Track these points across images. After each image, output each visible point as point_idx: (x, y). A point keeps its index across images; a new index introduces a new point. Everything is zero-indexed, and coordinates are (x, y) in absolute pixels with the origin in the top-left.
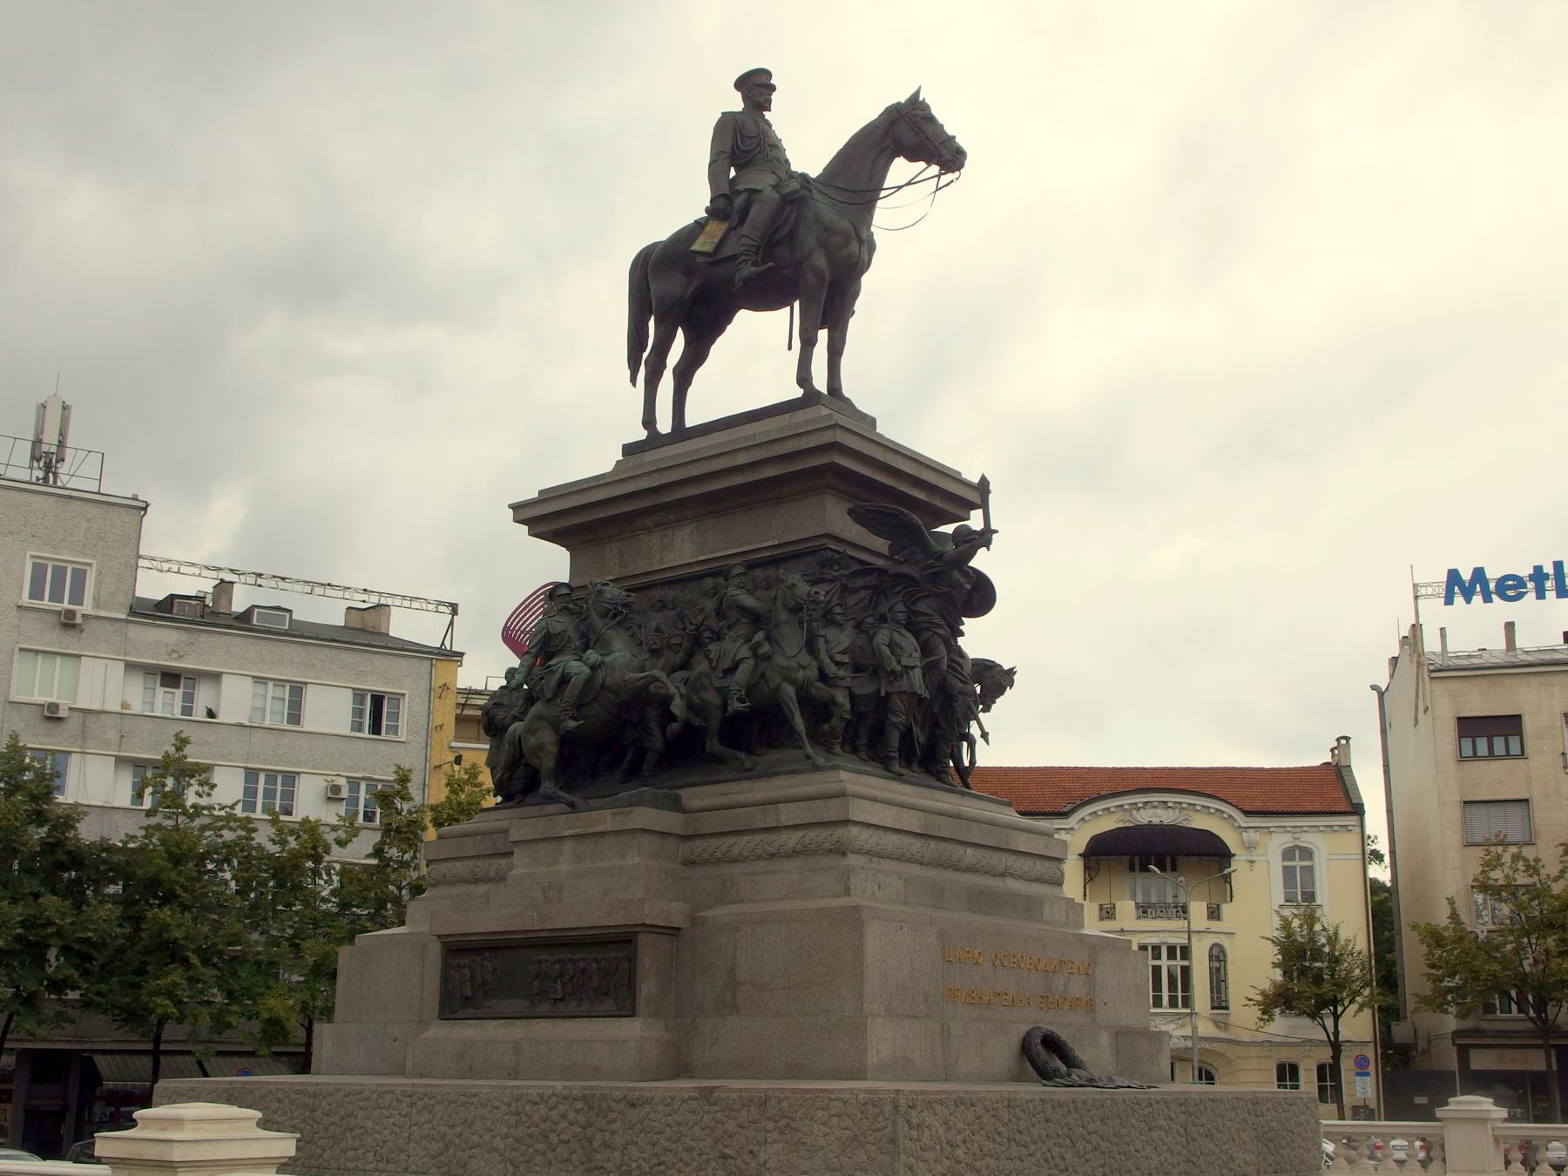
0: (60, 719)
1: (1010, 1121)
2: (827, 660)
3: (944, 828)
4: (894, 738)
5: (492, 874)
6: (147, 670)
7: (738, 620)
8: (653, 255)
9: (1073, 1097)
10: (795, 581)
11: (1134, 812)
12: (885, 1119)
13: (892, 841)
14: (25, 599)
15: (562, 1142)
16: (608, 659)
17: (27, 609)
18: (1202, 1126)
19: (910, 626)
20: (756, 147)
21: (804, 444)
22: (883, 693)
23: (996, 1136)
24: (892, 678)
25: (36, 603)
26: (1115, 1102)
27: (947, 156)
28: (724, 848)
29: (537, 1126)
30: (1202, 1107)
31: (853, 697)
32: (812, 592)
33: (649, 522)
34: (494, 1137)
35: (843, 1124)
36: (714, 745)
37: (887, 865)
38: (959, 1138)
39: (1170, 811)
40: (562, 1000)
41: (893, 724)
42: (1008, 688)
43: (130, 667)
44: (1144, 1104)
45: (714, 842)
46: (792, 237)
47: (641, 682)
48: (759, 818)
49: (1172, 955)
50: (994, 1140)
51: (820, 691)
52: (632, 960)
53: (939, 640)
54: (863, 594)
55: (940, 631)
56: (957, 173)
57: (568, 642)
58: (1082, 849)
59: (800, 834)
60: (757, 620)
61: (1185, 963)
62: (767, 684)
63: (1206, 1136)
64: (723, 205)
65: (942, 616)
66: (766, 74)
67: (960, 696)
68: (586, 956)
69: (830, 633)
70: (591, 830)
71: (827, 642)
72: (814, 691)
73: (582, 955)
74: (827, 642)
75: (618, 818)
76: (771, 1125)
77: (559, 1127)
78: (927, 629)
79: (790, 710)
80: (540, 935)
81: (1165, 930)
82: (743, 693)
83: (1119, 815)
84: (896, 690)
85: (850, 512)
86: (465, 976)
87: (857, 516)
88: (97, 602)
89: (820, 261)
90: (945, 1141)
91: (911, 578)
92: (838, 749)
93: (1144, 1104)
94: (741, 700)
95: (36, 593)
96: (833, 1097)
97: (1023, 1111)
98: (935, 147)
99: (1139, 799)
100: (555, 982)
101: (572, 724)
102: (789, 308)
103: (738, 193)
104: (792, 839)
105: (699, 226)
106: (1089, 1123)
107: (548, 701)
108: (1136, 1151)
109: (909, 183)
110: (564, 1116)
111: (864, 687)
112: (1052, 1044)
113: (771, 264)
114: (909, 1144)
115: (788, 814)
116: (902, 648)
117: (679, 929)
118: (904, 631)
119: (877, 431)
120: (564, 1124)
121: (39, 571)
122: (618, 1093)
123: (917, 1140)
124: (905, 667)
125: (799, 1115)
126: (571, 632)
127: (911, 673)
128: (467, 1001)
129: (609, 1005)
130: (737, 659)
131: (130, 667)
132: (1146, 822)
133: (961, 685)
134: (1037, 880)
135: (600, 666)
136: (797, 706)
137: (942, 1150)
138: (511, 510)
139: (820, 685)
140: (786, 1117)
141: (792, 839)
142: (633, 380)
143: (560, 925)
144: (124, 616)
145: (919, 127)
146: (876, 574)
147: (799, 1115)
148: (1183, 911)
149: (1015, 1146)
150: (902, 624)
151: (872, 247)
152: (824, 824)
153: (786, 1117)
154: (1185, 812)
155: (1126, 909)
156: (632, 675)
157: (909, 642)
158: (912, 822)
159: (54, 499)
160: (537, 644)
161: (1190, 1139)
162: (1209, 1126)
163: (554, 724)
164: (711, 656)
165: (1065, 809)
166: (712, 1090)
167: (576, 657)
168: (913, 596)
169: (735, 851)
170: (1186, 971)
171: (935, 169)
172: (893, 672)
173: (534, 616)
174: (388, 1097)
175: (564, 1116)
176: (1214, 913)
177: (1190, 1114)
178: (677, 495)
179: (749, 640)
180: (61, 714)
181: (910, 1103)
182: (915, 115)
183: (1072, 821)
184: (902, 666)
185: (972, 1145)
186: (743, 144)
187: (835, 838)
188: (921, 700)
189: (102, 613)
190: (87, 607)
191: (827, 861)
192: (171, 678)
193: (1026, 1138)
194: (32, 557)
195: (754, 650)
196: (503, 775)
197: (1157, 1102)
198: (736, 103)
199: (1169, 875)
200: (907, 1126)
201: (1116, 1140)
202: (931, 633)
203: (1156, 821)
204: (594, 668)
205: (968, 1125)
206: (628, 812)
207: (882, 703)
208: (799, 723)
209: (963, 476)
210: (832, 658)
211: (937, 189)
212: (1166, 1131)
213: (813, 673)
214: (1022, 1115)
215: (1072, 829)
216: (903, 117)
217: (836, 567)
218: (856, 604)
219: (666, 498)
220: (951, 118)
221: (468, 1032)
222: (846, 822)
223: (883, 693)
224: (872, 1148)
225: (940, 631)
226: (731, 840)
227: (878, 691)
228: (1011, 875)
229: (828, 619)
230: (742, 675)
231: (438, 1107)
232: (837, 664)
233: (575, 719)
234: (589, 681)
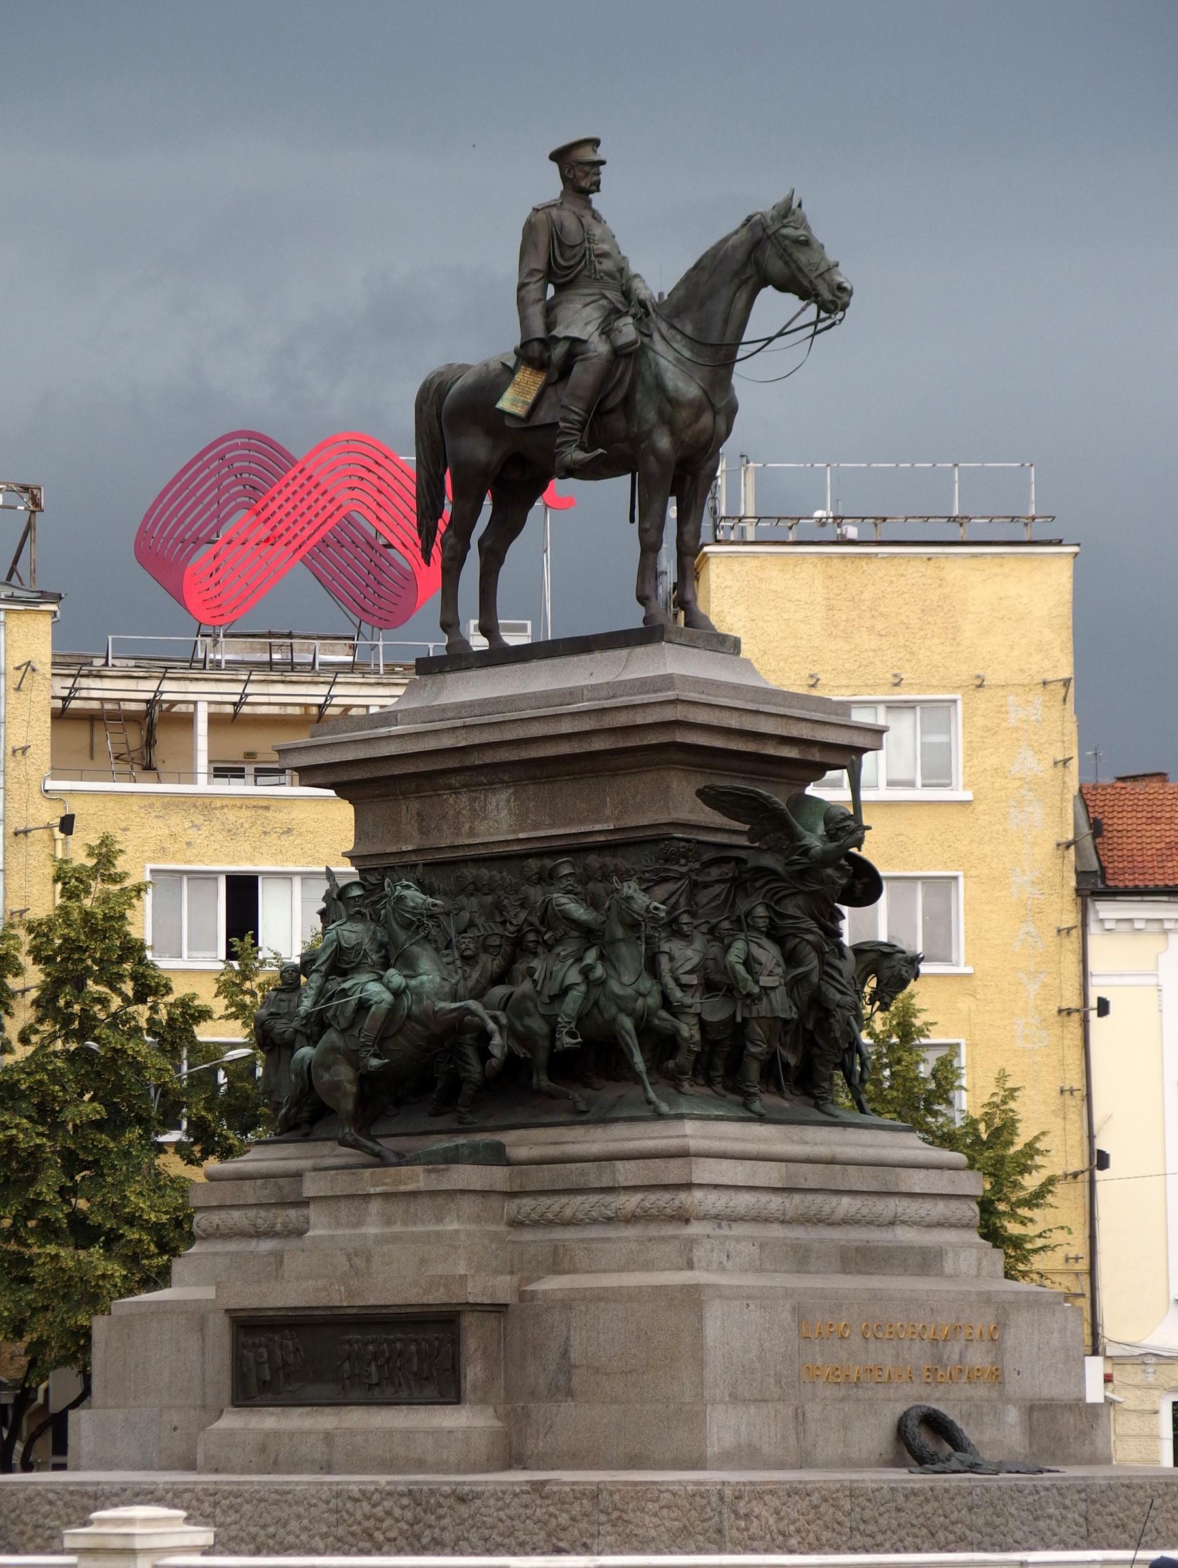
1: (852, 1510)
2: (671, 984)
3: (812, 1176)
5: (278, 1227)
7: (566, 934)
8: (451, 391)
9: (932, 1484)
10: (631, 892)
12: (712, 1510)
13: (743, 1202)
15: (388, 1540)
16: (413, 982)
18: (1111, 1515)
19: (775, 935)
20: (580, 262)
21: (640, 719)
22: (739, 1019)
23: (836, 1526)
24: (748, 1002)
26: (987, 1490)
28: (556, 1208)
29: (360, 1524)
30: (1110, 1494)
31: (703, 1025)
32: (652, 906)
33: (454, 781)
34: (312, 1537)
35: (673, 1515)
36: (542, 1081)
37: (739, 1230)
38: (792, 1528)
40: (377, 1384)
41: (752, 1055)
42: (913, 980)
44: (1027, 1492)
45: (545, 1201)
46: (628, 402)
47: (454, 1014)
48: (595, 1176)
50: (834, 1530)
52: (456, 1342)
53: (808, 948)
54: (717, 889)
55: (810, 937)
59: (639, 1197)
62: (601, 1013)
63: (1117, 1527)
65: (814, 918)
67: (839, 1010)
68: (403, 1336)
69: (675, 947)
70: (402, 1188)
71: (672, 959)
72: (657, 1022)
73: (399, 1335)
74: (672, 959)
75: (433, 1176)
76: (603, 1518)
77: (385, 1525)
78: (795, 936)
80: (349, 1311)
82: (573, 1025)
84: (755, 1015)
87: (708, 796)
89: (664, 442)
90: (776, 1531)
91: (774, 872)
93: (1027, 1492)
94: (572, 1035)
96: (662, 1488)
97: (869, 1500)
100: (369, 1365)
101: (375, 1062)
102: (630, 475)
103: (556, 340)
104: (631, 1202)
105: (509, 372)
106: (952, 1512)
107: (343, 1031)
108: (1016, 1542)
109: (780, 334)
111: (716, 1011)
112: (936, 1424)
114: (735, 1533)
115: (626, 1173)
116: (761, 964)
117: (506, 1305)
118: (765, 942)
120: (389, 1522)
122: (447, 1488)
123: (744, 1530)
124: (765, 988)
125: (631, 1506)
126: (367, 945)
127: (772, 995)
129: (430, 1391)
130: (567, 983)
133: (838, 996)
134: (939, 1225)
135: (404, 991)
136: (636, 1041)
137: (773, 1540)
139: (663, 1014)
140: (618, 1509)
141: (631, 1202)
142: (427, 555)
143: (372, 1302)
145: (790, 255)
146: (733, 863)
147: (631, 1506)
149: (858, 1536)
150: (762, 932)
152: (665, 1187)
153: (618, 1509)
157: (768, 954)
158: (769, 1174)
160: (326, 961)
161: (1092, 1529)
162: (1121, 1515)
163: (353, 1059)
164: (536, 977)
166: (544, 1483)
167: (374, 976)
168: (776, 893)
169: (568, 1212)
172: (749, 995)
173: (201, 507)
174: (187, 1496)
175: (389, 1513)
177: (1093, 1502)
178: (489, 758)
179: (579, 959)
181: (737, 1494)
182: (786, 237)
184: (761, 987)
185: (808, 1535)
186: (562, 256)
187: (677, 1203)
191: (669, 1230)
193: (872, 1528)
195: (586, 972)
196: (289, 1110)
197: (1047, 1489)
198: (550, 187)
200: (733, 1516)
201: (989, 1530)
202: (798, 940)
204: (397, 993)
205: (803, 1514)
206: (447, 1170)
207: (738, 1030)
210: (676, 980)
212: (1057, 1521)
213: (654, 1000)
214: (868, 1504)
216: (769, 237)
217: (683, 861)
218: (708, 903)
219: (476, 760)
222: (689, 1186)
223: (739, 1019)
224: (701, 1538)
225: (810, 937)
226: (564, 1200)
227: (734, 1015)
228: (904, 1222)
229: (674, 929)
231: (247, 1507)
232: (684, 987)
234: (393, 1010)
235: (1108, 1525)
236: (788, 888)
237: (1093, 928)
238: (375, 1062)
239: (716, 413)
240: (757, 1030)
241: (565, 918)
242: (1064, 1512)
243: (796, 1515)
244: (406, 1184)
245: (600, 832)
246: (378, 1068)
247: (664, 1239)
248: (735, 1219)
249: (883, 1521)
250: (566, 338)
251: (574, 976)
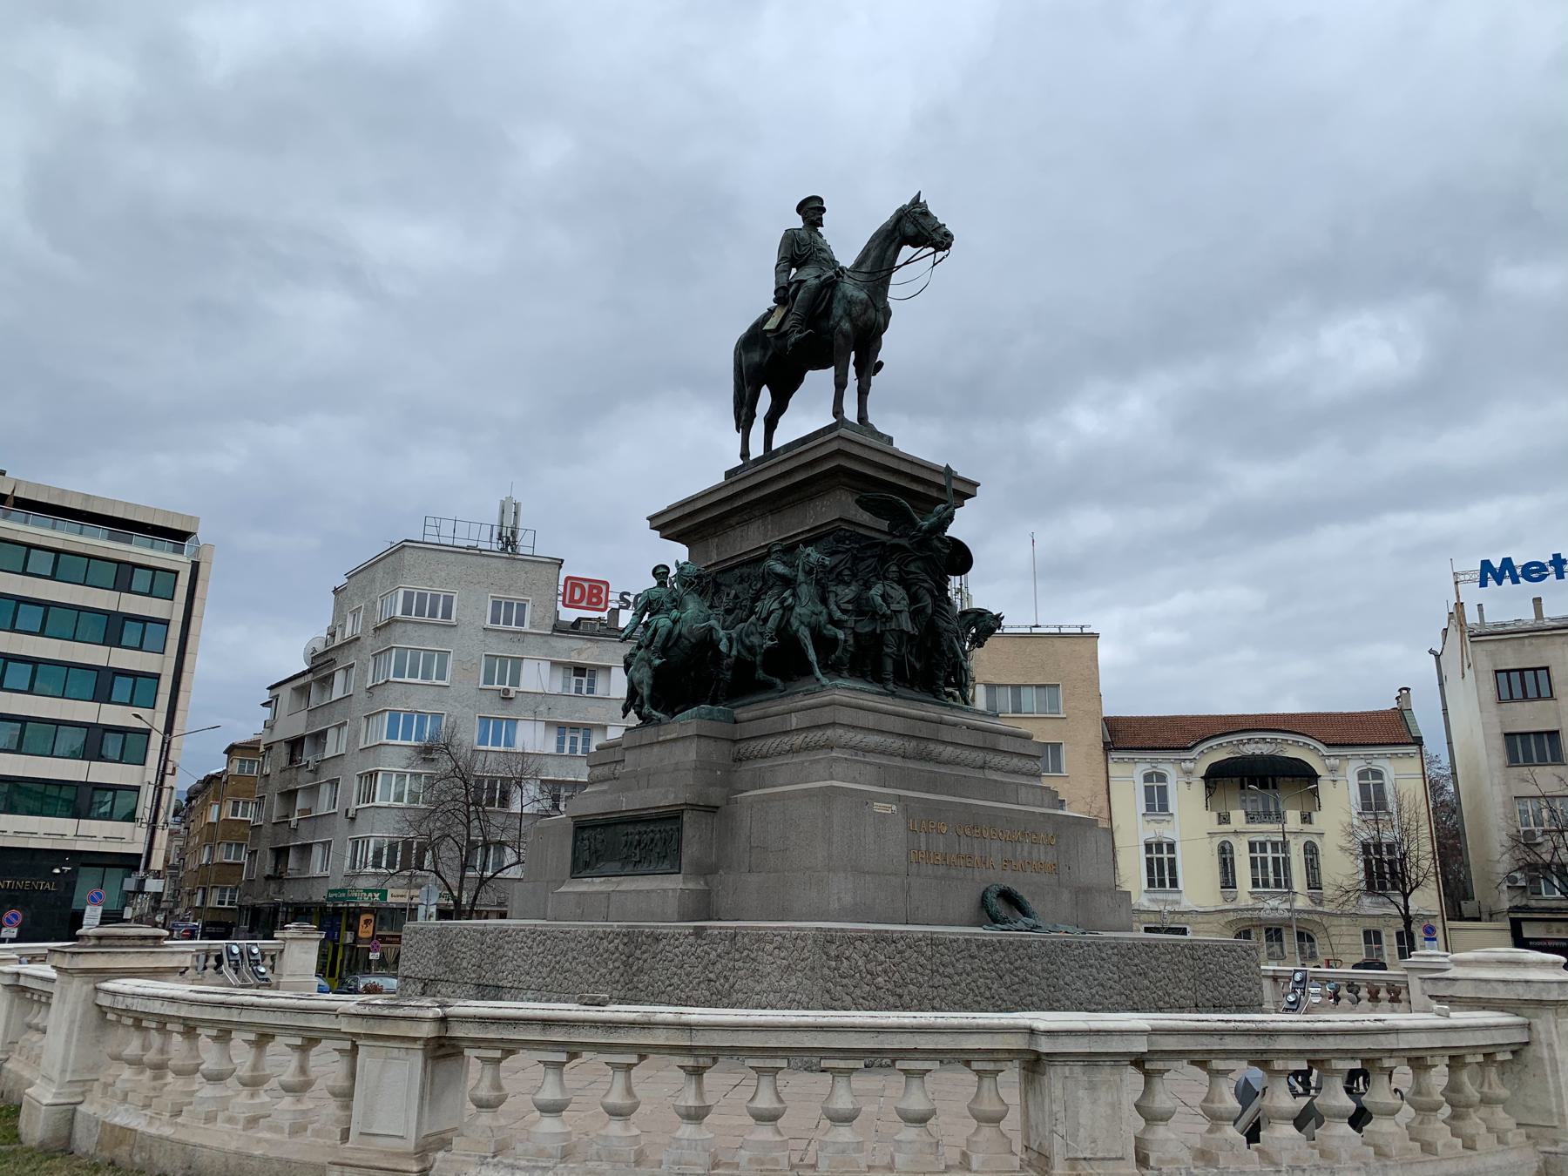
0: (511, 698)
1: (933, 956)
2: (835, 608)
3: (924, 730)
4: (889, 665)
6: (565, 666)
7: (774, 583)
9: (1000, 938)
10: (810, 551)
11: (1241, 746)
12: (808, 951)
13: (873, 740)
14: (488, 624)
15: (615, 968)
17: (490, 630)
18: (1136, 965)
19: (901, 581)
22: (878, 631)
23: (919, 968)
24: (884, 620)
25: (495, 626)
26: (1043, 944)
27: (939, 240)
30: (1135, 951)
31: (856, 635)
32: (820, 560)
33: (733, 521)
34: (577, 964)
35: (782, 955)
37: (870, 758)
38: (880, 968)
39: (1268, 744)
40: (640, 862)
41: (887, 655)
43: (554, 664)
44: (1074, 946)
46: (828, 312)
49: (1275, 849)
50: (916, 971)
51: (830, 630)
52: (680, 830)
53: (924, 592)
54: (869, 561)
55: (926, 585)
56: (947, 251)
57: (662, 605)
58: (1203, 774)
60: (788, 582)
61: (1253, 855)
62: (791, 627)
63: (1140, 974)
64: (783, 295)
65: (928, 574)
66: (820, 200)
67: (946, 633)
69: (840, 589)
71: (837, 595)
72: (825, 632)
74: (837, 595)
75: (684, 727)
76: (737, 956)
78: (916, 584)
79: (805, 645)
80: (627, 814)
81: (1267, 830)
83: (1230, 748)
84: (888, 628)
85: (858, 502)
86: (585, 845)
87: (863, 504)
88: (532, 625)
89: (846, 325)
90: (864, 970)
91: (904, 547)
92: (845, 674)
93: (1074, 946)
94: (771, 639)
95: (495, 620)
96: (776, 933)
97: (947, 949)
98: (929, 233)
99: (1245, 737)
100: (635, 849)
104: (798, 740)
105: (771, 312)
106: (1016, 960)
108: (1066, 984)
110: (617, 948)
111: (865, 628)
112: (1008, 897)
114: (826, 971)
116: (892, 598)
117: (717, 807)
118: (895, 586)
119: (894, 446)
120: (617, 955)
121: (496, 605)
122: (647, 930)
123: (835, 969)
124: (894, 611)
125: (755, 947)
126: (664, 599)
127: (899, 616)
128: (587, 865)
129: (666, 866)
131: (554, 664)
132: (1250, 753)
133: (945, 624)
134: (1014, 772)
135: (678, 620)
136: (811, 642)
137: (862, 978)
138: (648, 521)
139: (829, 626)
140: (747, 949)
141: (798, 740)
144: (550, 633)
145: (917, 221)
146: (880, 547)
147: (755, 947)
148: (1280, 817)
149: (938, 977)
150: (895, 581)
151: (887, 313)
152: (818, 727)
153: (747, 949)
154: (1279, 746)
155: (1238, 817)
156: (697, 625)
157: (898, 592)
158: (898, 725)
159: (505, 560)
161: (1122, 976)
162: (1143, 966)
165: (1189, 745)
166: (704, 928)
168: (903, 561)
170: (1287, 861)
171: (931, 250)
172: (884, 615)
174: (522, 933)
176: (1306, 819)
177: (1123, 956)
178: (746, 499)
180: (510, 696)
181: (828, 938)
182: (915, 212)
183: (1194, 754)
184: (892, 611)
185: (893, 975)
186: (799, 250)
187: (826, 737)
188: (911, 637)
189: (534, 631)
190: (526, 627)
191: (821, 755)
192: (580, 670)
193: (950, 970)
194: (492, 597)
195: (782, 603)
197: (1088, 945)
198: (798, 222)
199: (1269, 793)
200: (825, 957)
201: (1045, 975)
202: (917, 587)
203: (1258, 752)
204: (675, 622)
205: (890, 958)
207: (878, 639)
209: (958, 474)
210: (839, 607)
211: (934, 265)
212: (1097, 968)
213: (823, 618)
214: (946, 951)
215: (1195, 759)
217: (847, 542)
218: (864, 569)
220: (939, 210)
223: (878, 631)
224: (799, 974)
225: (926, 585)
227: (875, 629)
228: (990, 768)
229: (840, 581)
230: (771, 623)
231: (548, 942)
232: (844, 612)
233: (661, 659)
234: (670, 632)
235: (1134, 973)
236: (911, 556)
237: (1110, 761)
239: (877, 311)
241: (773, 573)
242: (1102, 963)
243: (883, 958)
244: (671, 734)
245: (802, 533)
246: (659, 665)
247: (818, 761)
248: (867, 751)
249: (959, 966)
250: (796, 281)
251: (775, 605)
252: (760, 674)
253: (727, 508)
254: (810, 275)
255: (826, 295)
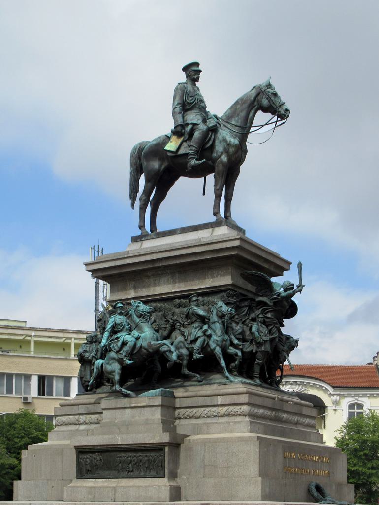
5: (87, 421)
16: (142, 335)
20: (194, 102)
21: (225, 245)
22: (254, 351)
33: (149, 274)
36: (186, 371)
45: (189, 410)
47: (158, 345)
51: (232, 350)
57: (124, 327)
59: (226, 408)
60: (203, 320)
68: (142, 455)
70: (139, 405)
72: (229, 350)
73: (140, 454)
75: (151, 400)
78: (271, 325)
79: (219, 358)
82: (200, 350)
85: (241, 275)
86: (87, 461)
94: (199, 353)
101: (130, 362)
103: (188, 124)
104: (223, 410)
105: (168, 138)
107: (117, 352)
112: (318, 488)
113: (204, 160)
115: (220, 400)
129: (153, 473)
130: (197, 336)
143: (131, 443)
146: (249, 301)
151: (246, 152)
156: (154, 342)
158: (269, 403)
160: (110, 328)
163: (120, 361)
164: (185, 334)
167: (128, 334)
169: (198, 414)
179: (201, 328)
196: (93, 381)
198: (182, 78)
204: (138, 339)
206: (157, 398)
208: (223, 363)
213: (228, 343)
221: (90, 483)
223: (254, 351)
226: (197, 410)
227: (253, 350)
230: (198, 344)
234: (135, 344)
236: (270, 308)
238: (130, 362)
239: (242, 151)
240: (259, 355)
241: (196, 314)
244: (140, 403)
245: (204, 288)
246: (131, 364)
250: (191, 124)
251: (200, 334)
252: (186, 371)
253: (150, 266)
254: (193, 117)
255: (211, 136)
